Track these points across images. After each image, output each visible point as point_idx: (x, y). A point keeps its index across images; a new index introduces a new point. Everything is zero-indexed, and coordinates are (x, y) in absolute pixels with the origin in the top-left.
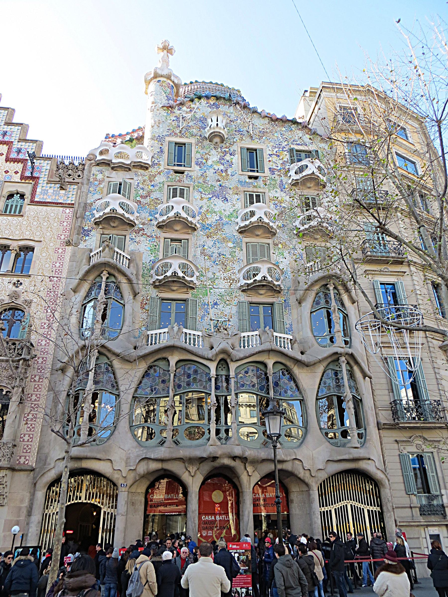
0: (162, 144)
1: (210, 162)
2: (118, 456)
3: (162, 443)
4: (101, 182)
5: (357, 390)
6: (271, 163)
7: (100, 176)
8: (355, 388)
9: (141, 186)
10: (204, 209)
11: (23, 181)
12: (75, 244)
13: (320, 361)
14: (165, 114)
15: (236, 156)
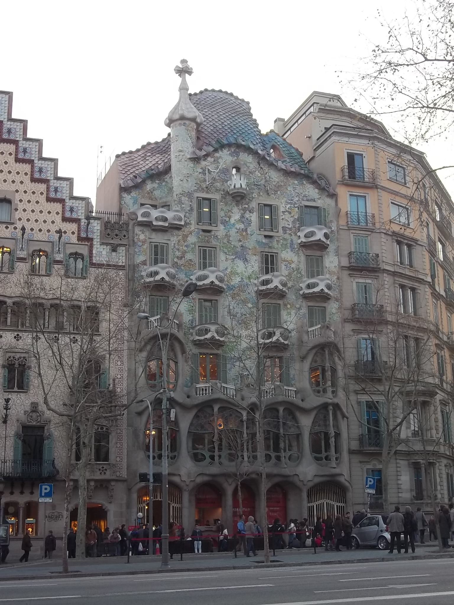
0: (191, 202)
1: (232, 221)
2: (183, 472)
3: (211, 464)
4: (144, 242)
5: (338, 427)
6: (284, 221)
7: (142, 237)
8: (336, 426)
9: (177, 247)
10: (229, 270)
11: (80, 243)
12: (131, 305)
13: (315, 408)
14: (192, 165)
15: (255, 213)
